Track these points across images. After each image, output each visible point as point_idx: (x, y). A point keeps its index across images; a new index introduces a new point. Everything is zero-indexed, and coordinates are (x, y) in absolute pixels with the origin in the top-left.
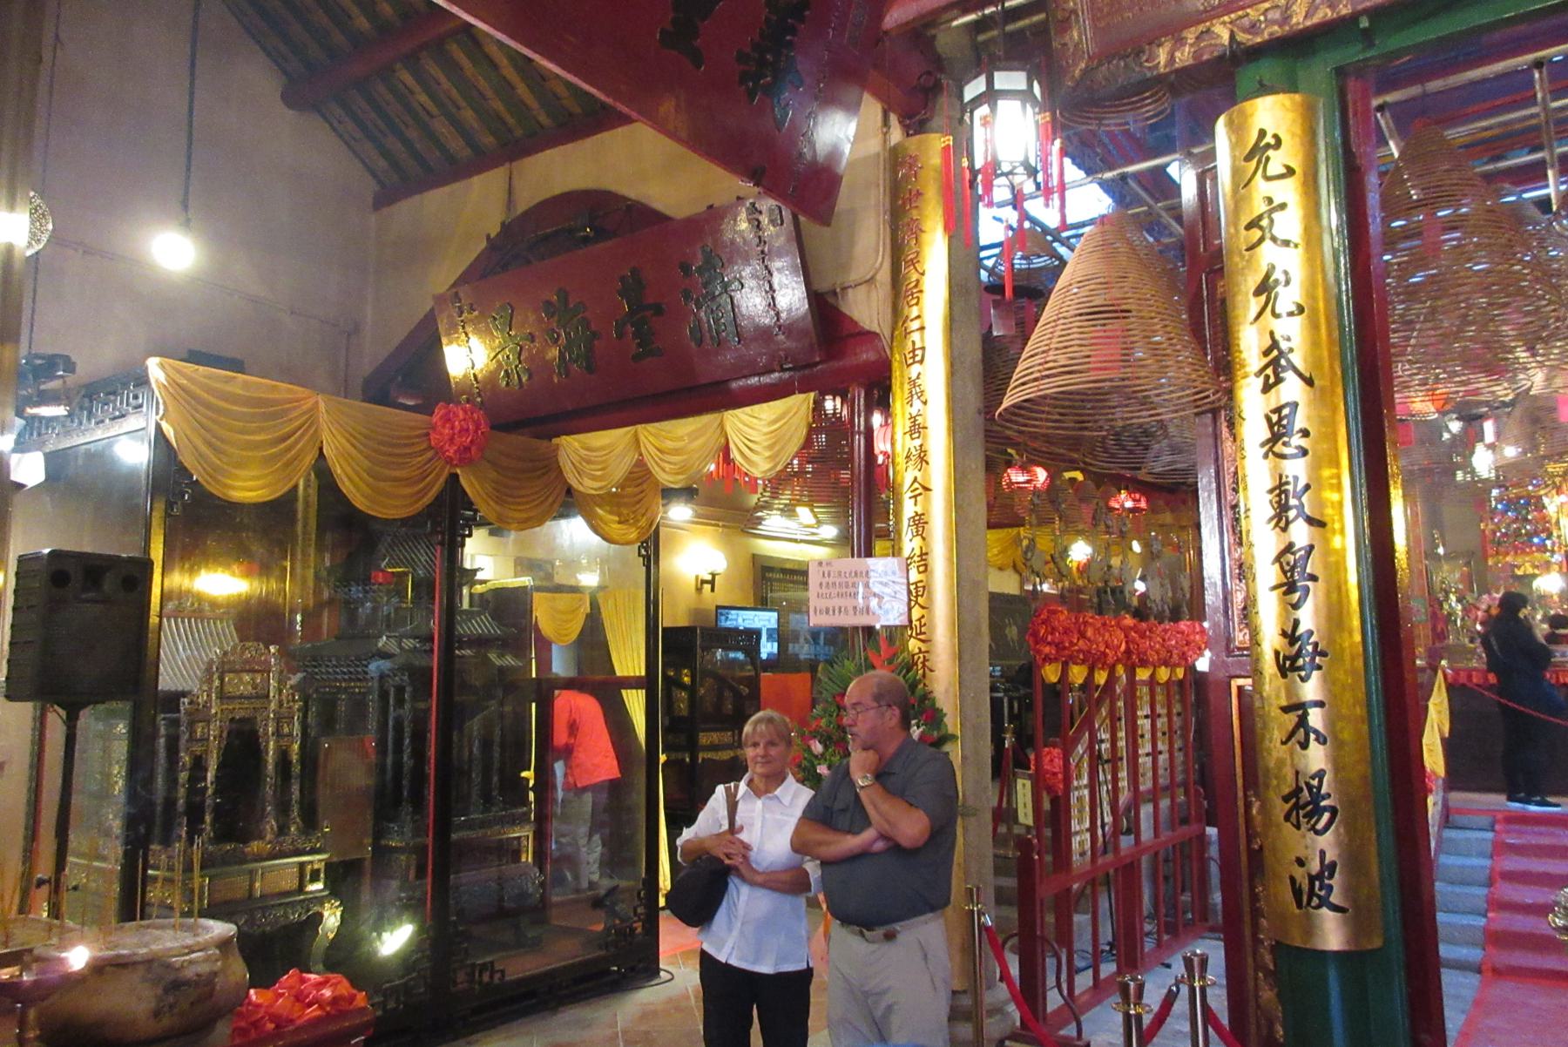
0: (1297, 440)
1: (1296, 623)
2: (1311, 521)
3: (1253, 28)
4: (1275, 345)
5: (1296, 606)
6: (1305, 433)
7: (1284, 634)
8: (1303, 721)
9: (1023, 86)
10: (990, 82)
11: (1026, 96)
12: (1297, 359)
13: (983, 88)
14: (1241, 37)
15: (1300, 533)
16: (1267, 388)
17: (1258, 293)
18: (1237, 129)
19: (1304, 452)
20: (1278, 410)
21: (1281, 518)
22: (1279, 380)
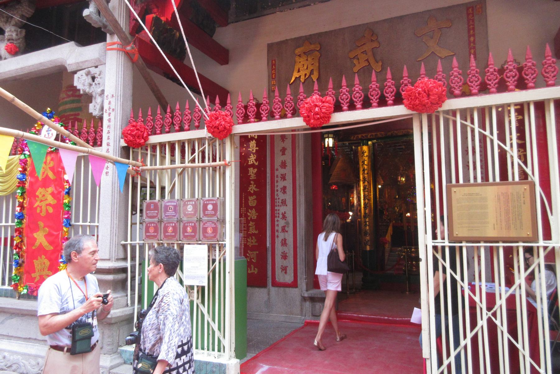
0: (367, 190)
1: (366, 212)
2: (368, 199)
3: (363, 137)
4: (364, 178)
5: (366, 209)
6: (368, 189)
7: (364, 213)
8: (366, 224)
9: (332, 136)
10: (328, 136)
11: (333, 138)
12: (367, 179)
13: (327, 136)
14: (362, 138)
15: (367, 201)
16: (364, 183)
17: (363, 171)
18: (362, 149)
19: (367, 191)
20: (365, 186)
21: (364, 199)
22: (365, 182)
